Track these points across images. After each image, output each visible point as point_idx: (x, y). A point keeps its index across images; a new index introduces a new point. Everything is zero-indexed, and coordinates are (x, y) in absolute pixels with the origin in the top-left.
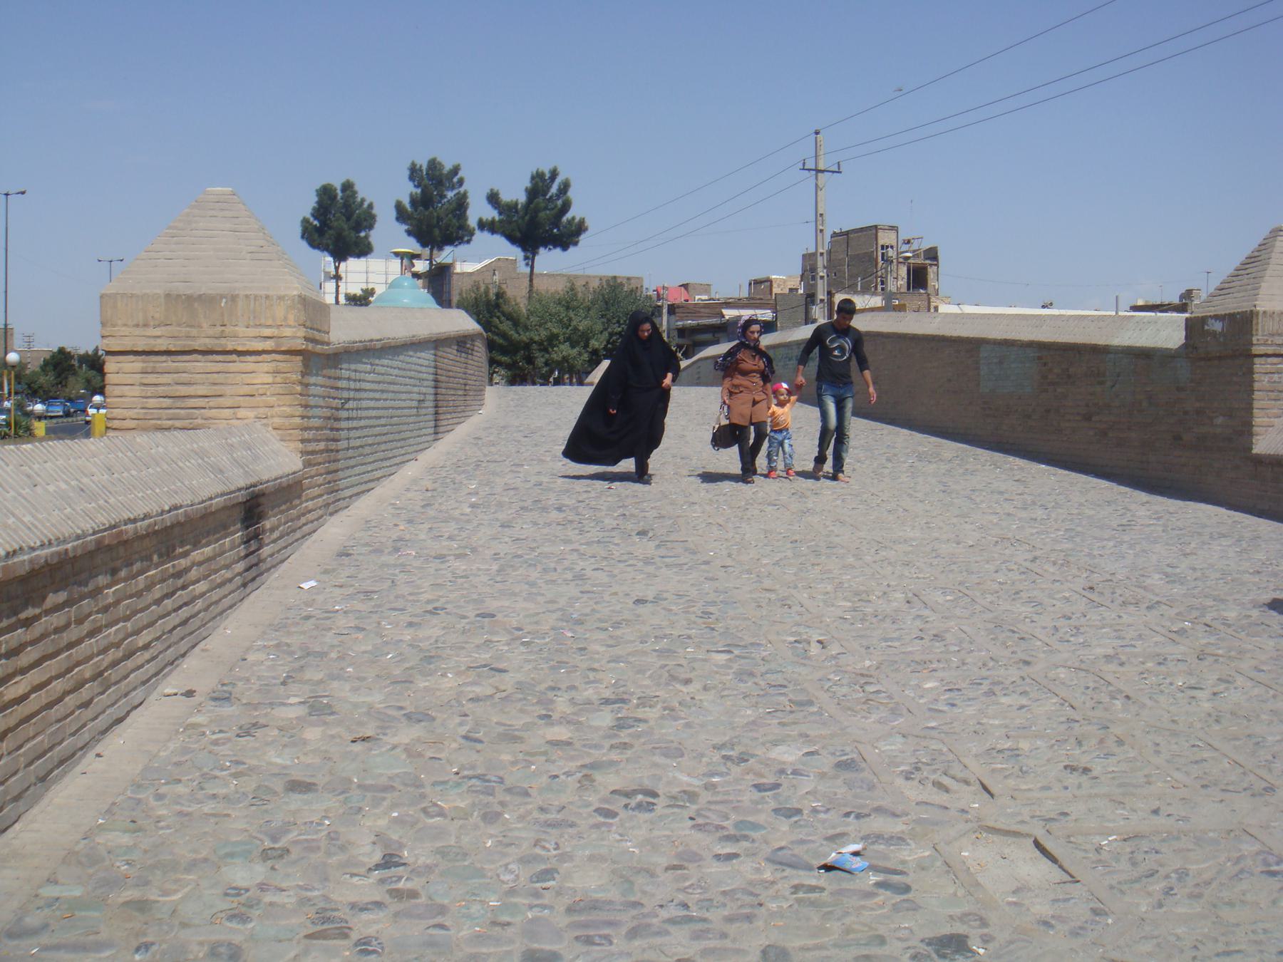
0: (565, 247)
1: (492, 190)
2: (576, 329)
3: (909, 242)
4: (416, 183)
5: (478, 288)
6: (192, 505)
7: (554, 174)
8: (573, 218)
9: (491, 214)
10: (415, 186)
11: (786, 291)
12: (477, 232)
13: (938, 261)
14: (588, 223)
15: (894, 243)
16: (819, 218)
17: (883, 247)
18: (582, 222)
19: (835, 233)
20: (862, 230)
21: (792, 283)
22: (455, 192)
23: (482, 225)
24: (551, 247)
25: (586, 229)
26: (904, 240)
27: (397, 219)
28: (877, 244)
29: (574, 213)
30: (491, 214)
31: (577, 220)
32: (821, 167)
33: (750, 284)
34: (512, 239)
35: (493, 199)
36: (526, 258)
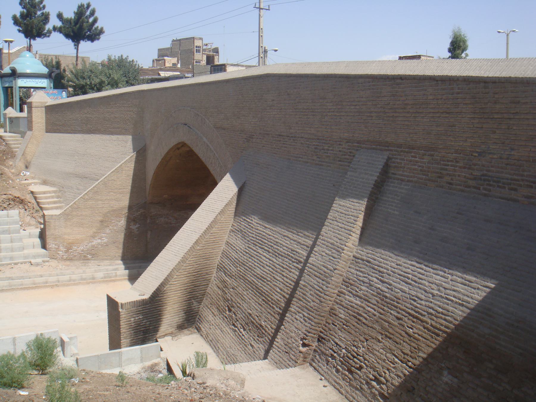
0: (92, 41)
1: (59, 12)
2: (113, 78)
3: (206, 45)
4: (23, 6)
5: (47, 59)
6: (518, 160)
7: (89, 6)
8: (98, 27)
9: (59, 24)
10: (22, 8)
11: (171, 65)
12: (53, 32)
13: (219, 53)
14: (104, 29)
15: (201, 45)
16: (261, 30)
17: (196, 47)
18: (102, 29)
19: (173, 40)
20: (187, 39)
21: (174, 61)
22: (41, 12)
23: (55, 29)
24: (86, 40)
25: (104, 32)
26: (204, 44)
27: (14, 24)
28: (194, 45)
29: (99, 25)
30: (59, 24)
31: (99, 28)
32: (262, 7)
33: (153, 61)
34: (67, 36)
35: (60, 16)
36: (75, 45)
